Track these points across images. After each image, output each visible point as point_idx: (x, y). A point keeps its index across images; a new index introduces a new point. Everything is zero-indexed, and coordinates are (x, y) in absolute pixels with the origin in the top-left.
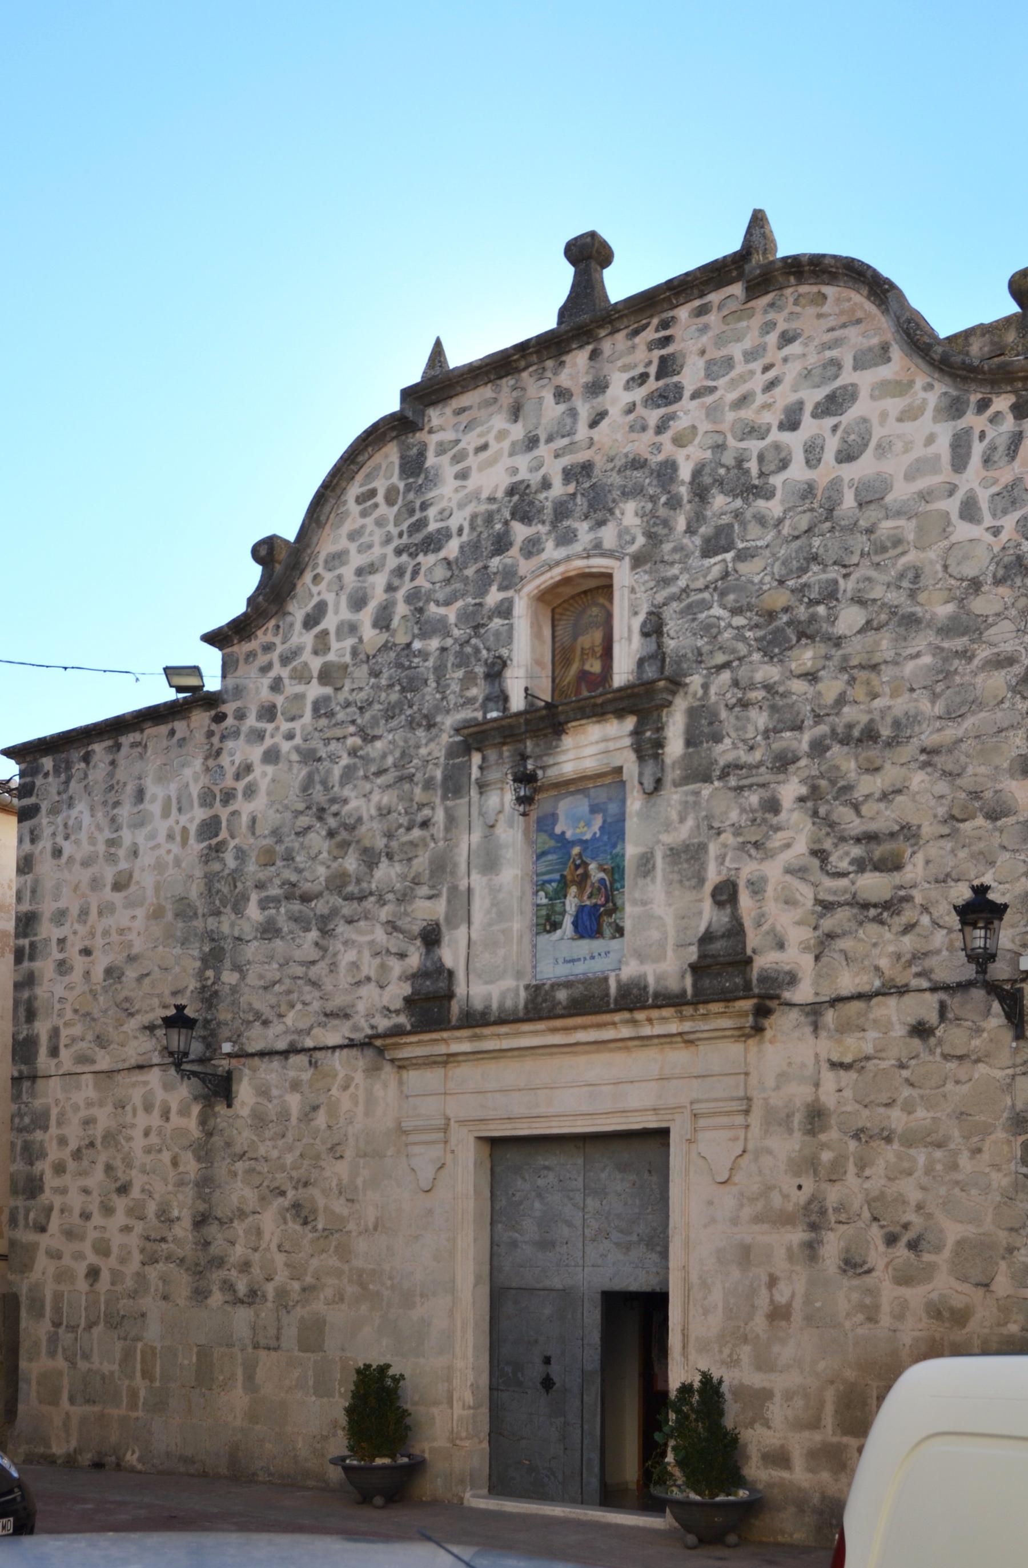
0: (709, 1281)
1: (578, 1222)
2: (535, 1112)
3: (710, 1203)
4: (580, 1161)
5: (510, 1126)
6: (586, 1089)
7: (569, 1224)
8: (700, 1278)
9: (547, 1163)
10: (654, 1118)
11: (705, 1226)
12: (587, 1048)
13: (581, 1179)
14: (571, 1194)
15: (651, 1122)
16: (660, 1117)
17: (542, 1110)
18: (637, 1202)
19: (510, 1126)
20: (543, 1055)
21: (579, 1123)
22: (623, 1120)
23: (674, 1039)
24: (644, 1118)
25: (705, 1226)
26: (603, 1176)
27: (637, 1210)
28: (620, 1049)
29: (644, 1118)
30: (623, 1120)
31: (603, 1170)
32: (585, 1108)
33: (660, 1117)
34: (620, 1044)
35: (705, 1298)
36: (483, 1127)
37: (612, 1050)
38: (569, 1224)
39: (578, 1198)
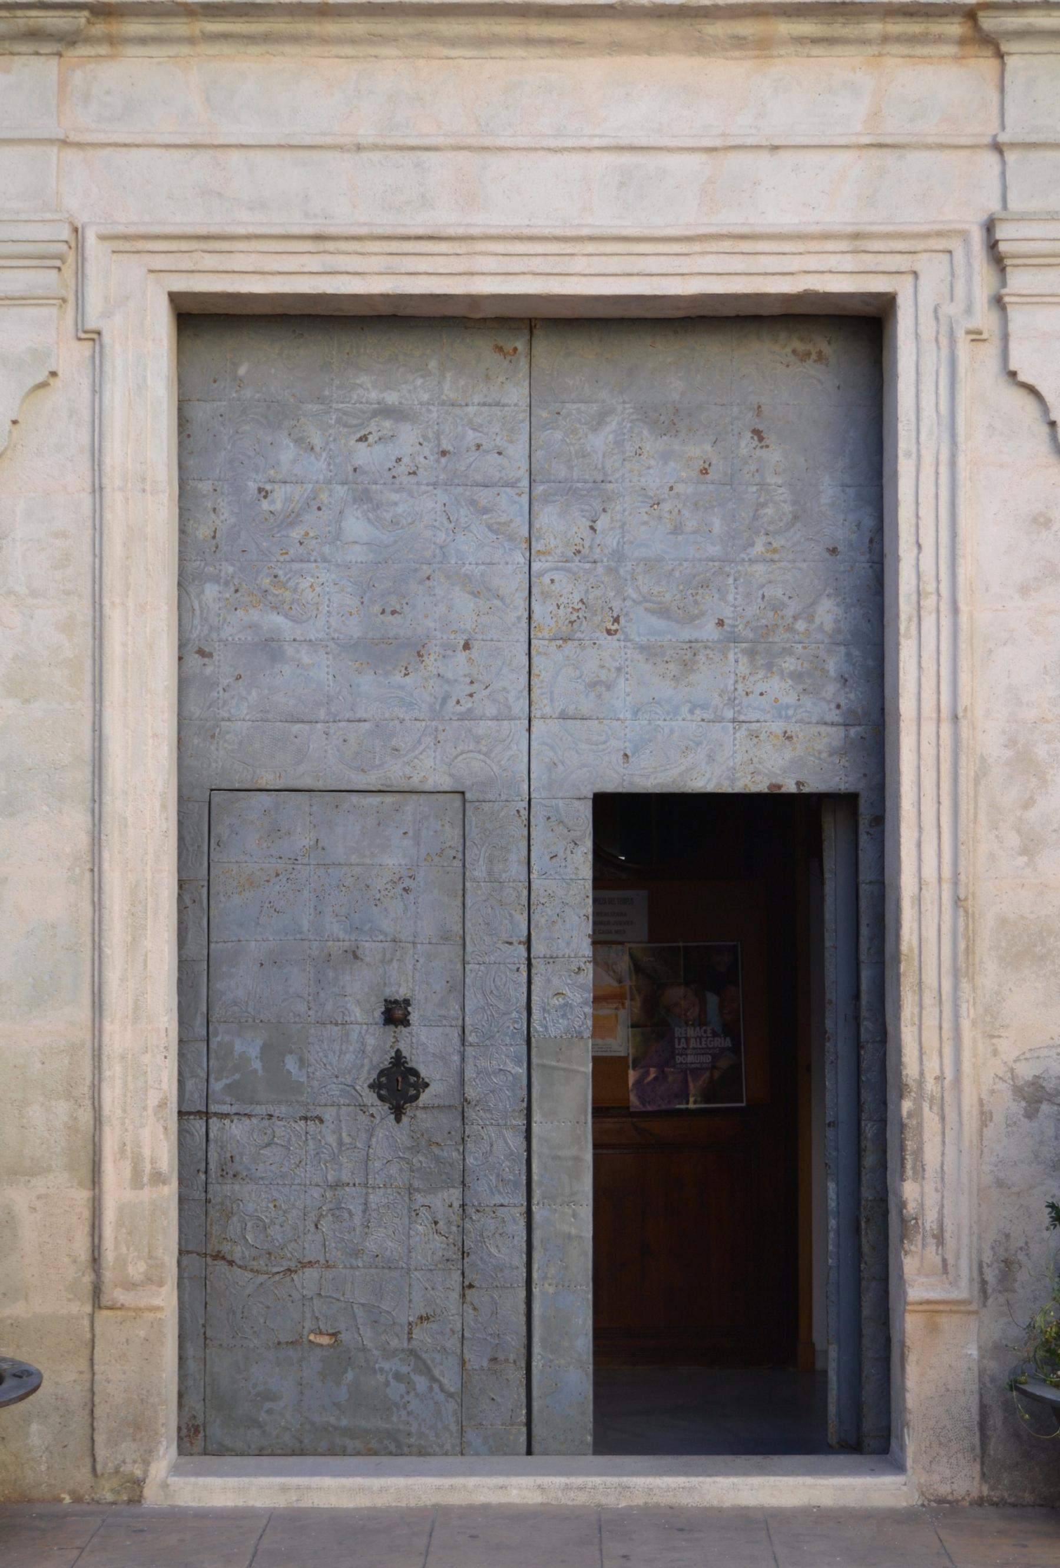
0: (1041, 751)
1: (513, 585)
2: (419, 222)
3: (1041, 522)
4: (516, 394)
5: (314, 264)
6: (608, 158)
7: (481, 590)
8: (1011, 742)
9: (391, 398)
10: (848, 263)
11: (1025, 590)
12: (654, 28)
13: (518, 450)
14: (484, 496)
15: (838, 277)
16: (868, 262)
17: (444, 217)
18: (717, 525)
19: (314, 264)
20: (452, 42)
21: (580, 264)
22: (738, 264)
23: (937, 28)
24: (812, 263)
25: (1025, 590)
26: (599, 441)
27: (714, 550)
28: (740, 43)
29: (812, 263)
30: (738, 264)
31: (599, 421)
32: (604, 218)
33: (868, 262)
34: (747, 28)
35: (1028, 804)
36: (210, 262)
37: (702, 48)
38: (481, 590)
39: (510, 507)
